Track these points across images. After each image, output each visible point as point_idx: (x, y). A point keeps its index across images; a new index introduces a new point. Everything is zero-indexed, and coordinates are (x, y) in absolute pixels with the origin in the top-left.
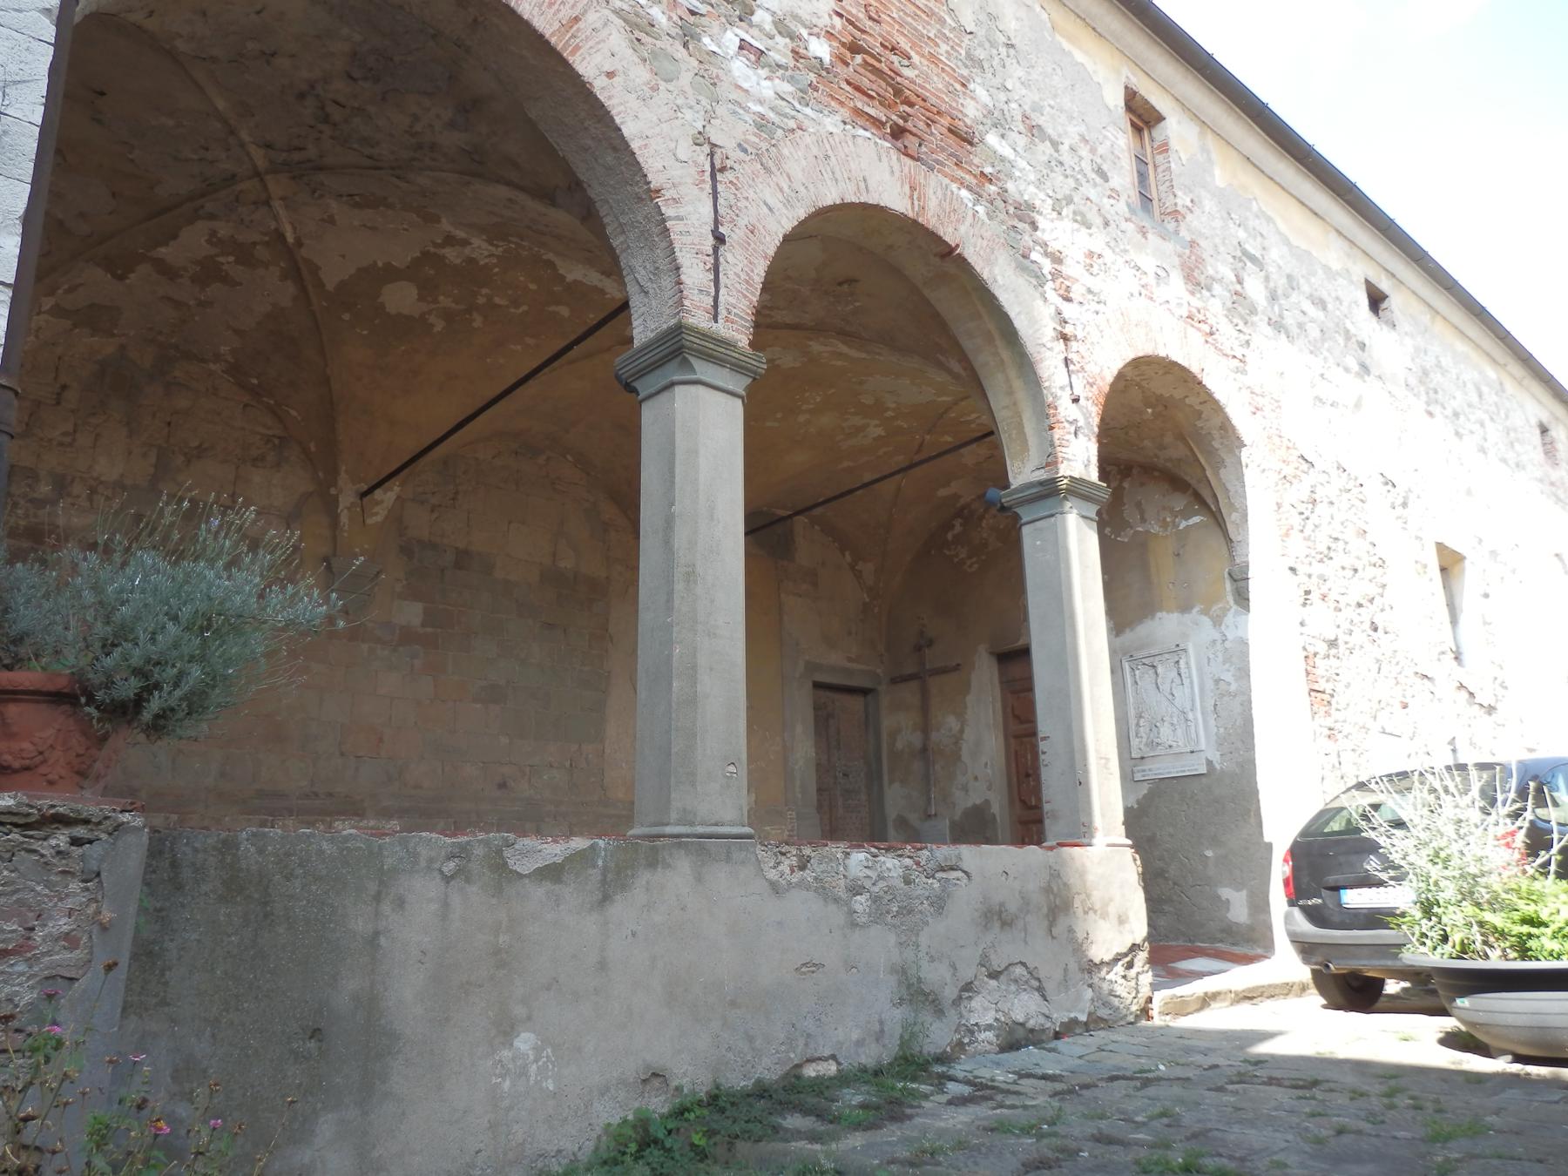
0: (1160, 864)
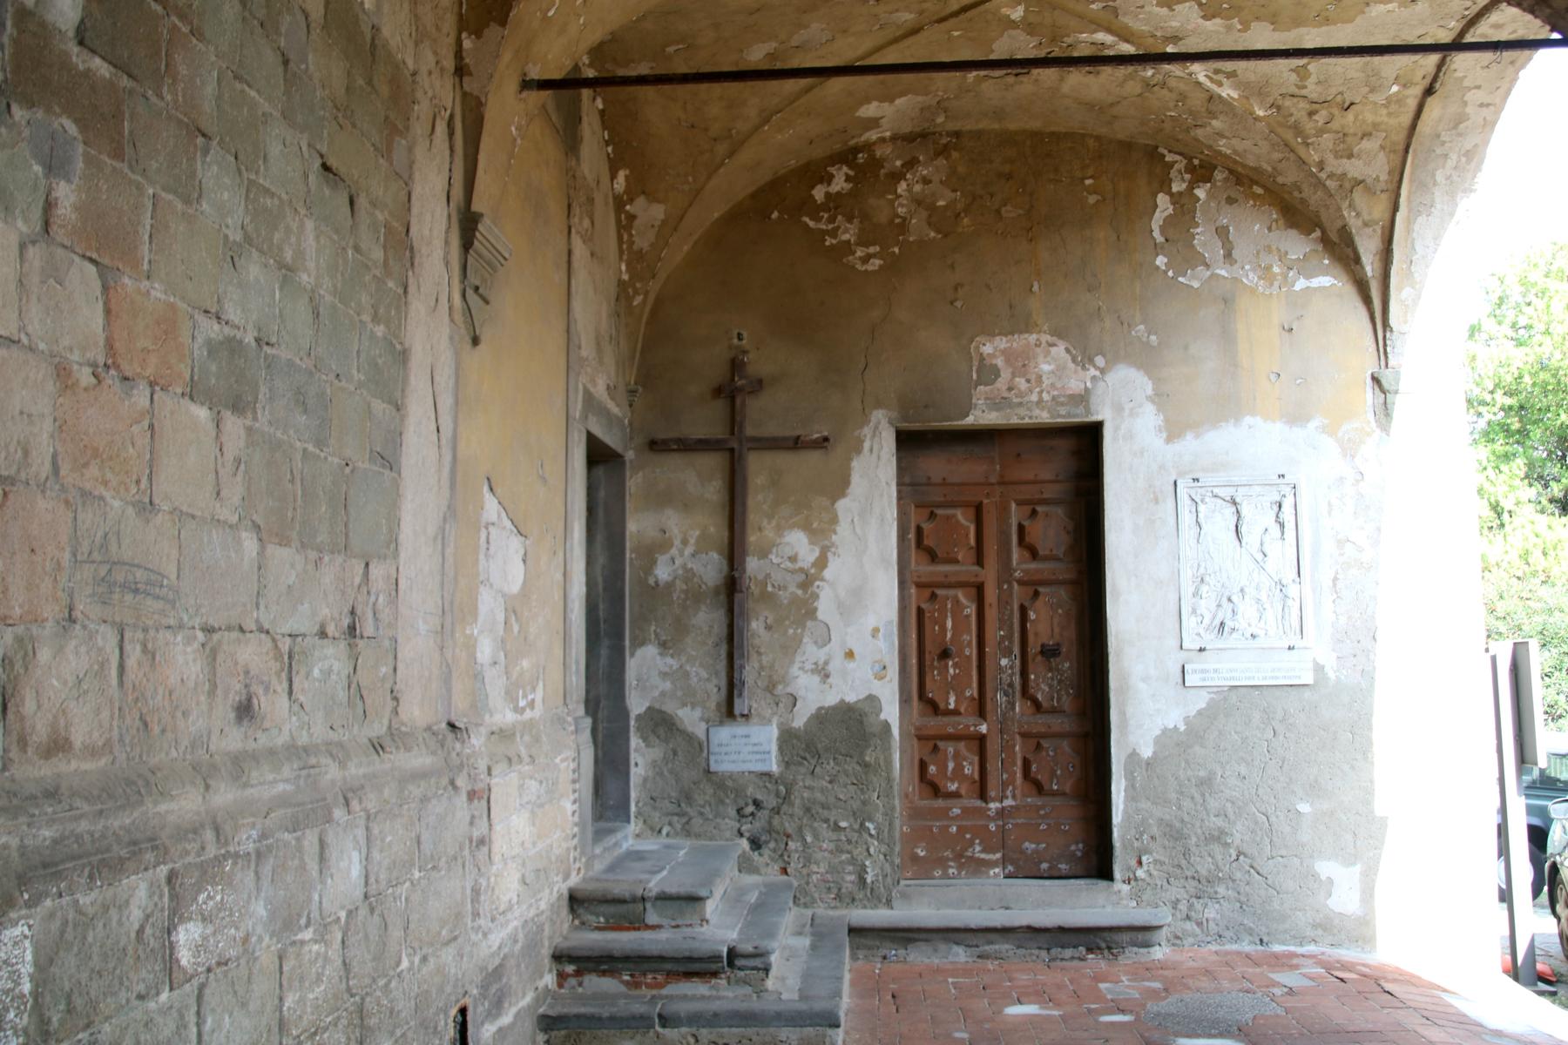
0: (1220, 822)
